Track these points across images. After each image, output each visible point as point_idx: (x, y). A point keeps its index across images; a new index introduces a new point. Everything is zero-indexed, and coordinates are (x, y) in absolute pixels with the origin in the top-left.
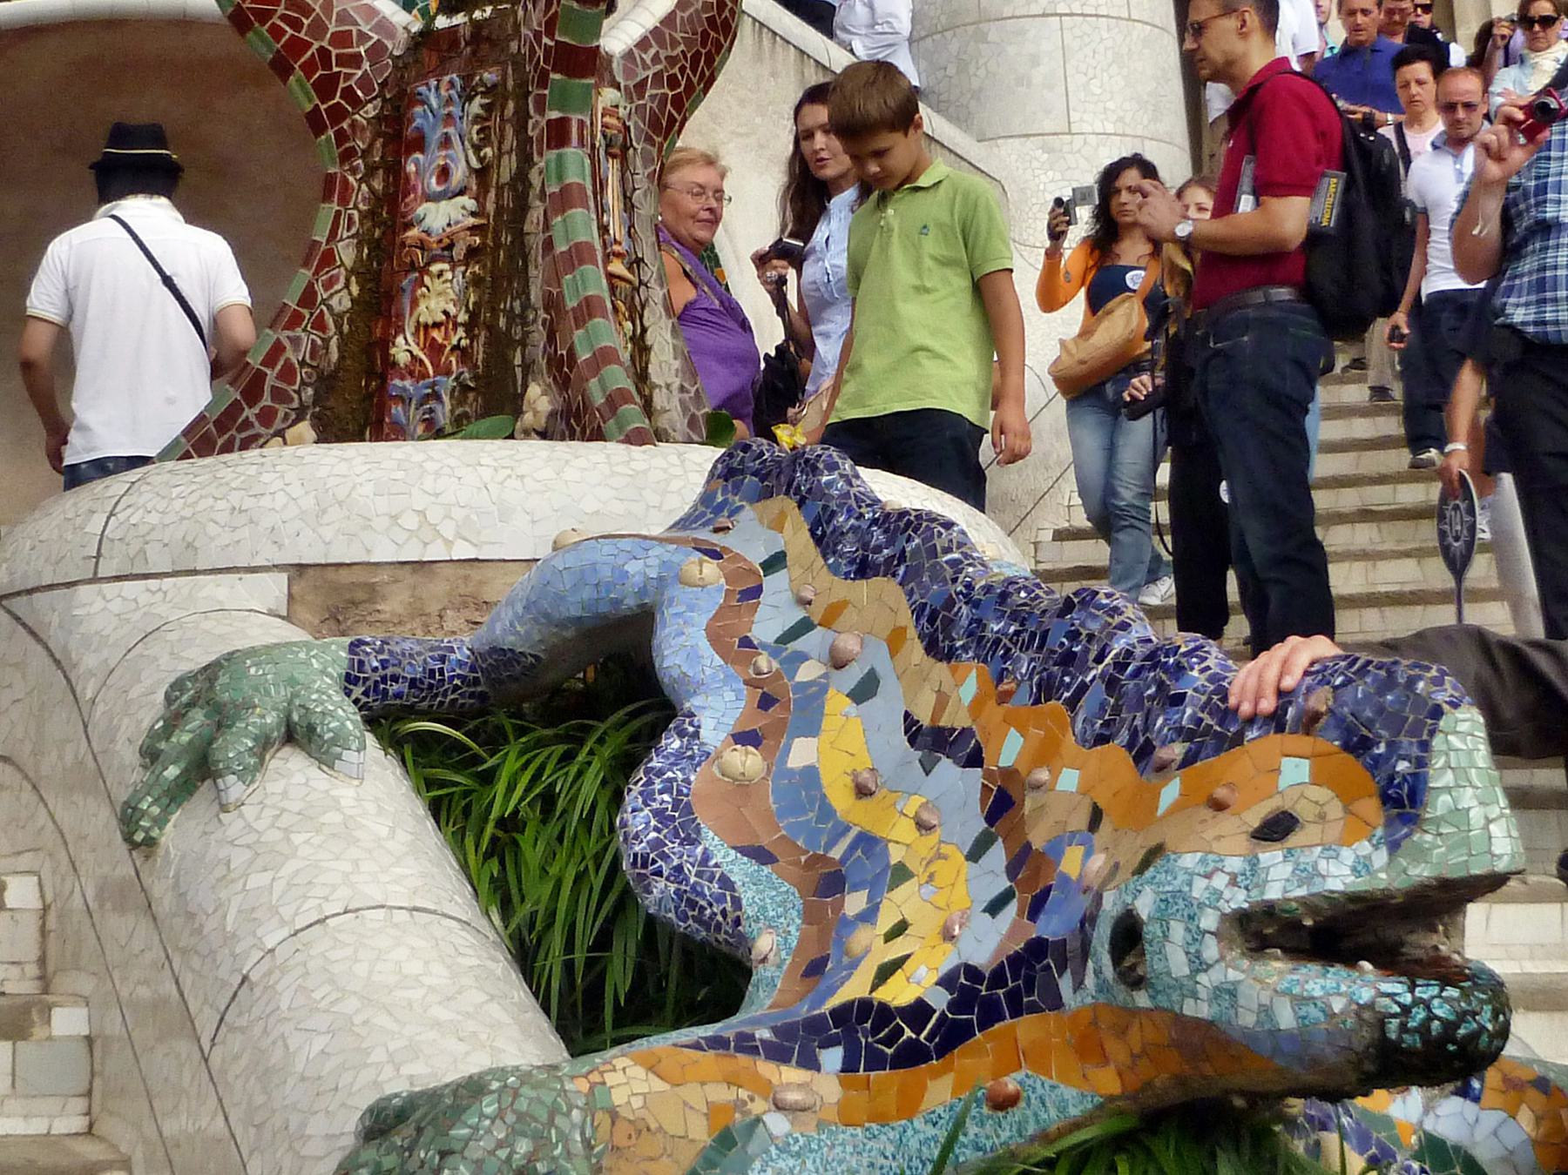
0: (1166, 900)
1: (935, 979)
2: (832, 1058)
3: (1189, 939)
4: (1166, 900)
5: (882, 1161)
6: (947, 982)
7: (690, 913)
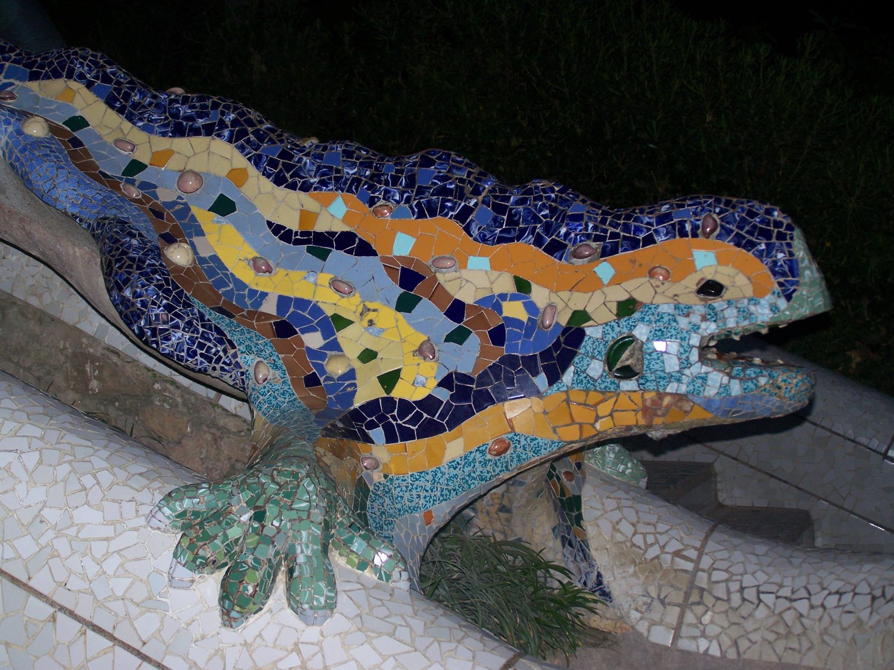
0: (660, 330)
1: (436, 383)
2: (377, 434)
3: (682, 351)
4: (660, 330)
5: (425, 493)
6: (446, 383)
7: (199, 351)
